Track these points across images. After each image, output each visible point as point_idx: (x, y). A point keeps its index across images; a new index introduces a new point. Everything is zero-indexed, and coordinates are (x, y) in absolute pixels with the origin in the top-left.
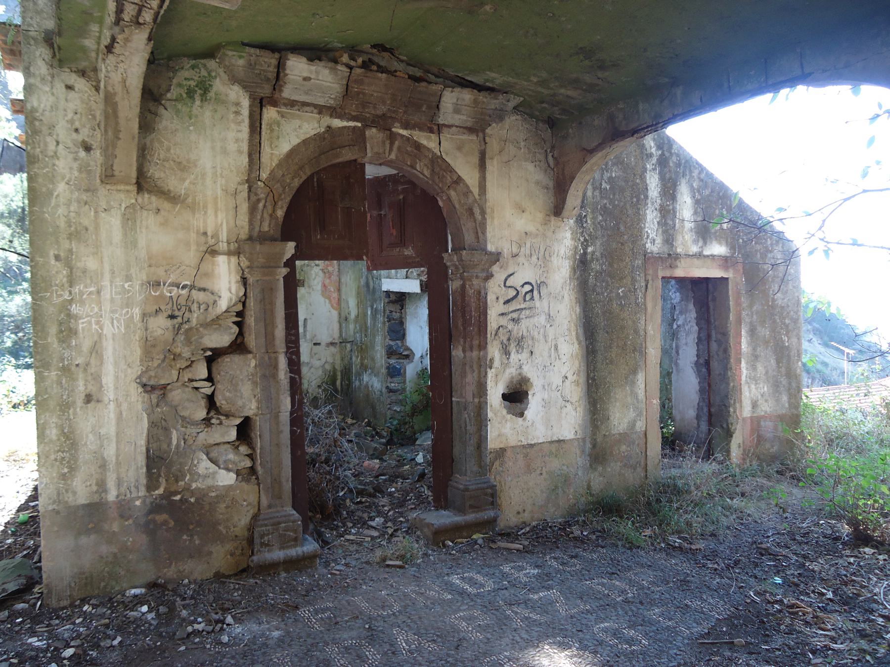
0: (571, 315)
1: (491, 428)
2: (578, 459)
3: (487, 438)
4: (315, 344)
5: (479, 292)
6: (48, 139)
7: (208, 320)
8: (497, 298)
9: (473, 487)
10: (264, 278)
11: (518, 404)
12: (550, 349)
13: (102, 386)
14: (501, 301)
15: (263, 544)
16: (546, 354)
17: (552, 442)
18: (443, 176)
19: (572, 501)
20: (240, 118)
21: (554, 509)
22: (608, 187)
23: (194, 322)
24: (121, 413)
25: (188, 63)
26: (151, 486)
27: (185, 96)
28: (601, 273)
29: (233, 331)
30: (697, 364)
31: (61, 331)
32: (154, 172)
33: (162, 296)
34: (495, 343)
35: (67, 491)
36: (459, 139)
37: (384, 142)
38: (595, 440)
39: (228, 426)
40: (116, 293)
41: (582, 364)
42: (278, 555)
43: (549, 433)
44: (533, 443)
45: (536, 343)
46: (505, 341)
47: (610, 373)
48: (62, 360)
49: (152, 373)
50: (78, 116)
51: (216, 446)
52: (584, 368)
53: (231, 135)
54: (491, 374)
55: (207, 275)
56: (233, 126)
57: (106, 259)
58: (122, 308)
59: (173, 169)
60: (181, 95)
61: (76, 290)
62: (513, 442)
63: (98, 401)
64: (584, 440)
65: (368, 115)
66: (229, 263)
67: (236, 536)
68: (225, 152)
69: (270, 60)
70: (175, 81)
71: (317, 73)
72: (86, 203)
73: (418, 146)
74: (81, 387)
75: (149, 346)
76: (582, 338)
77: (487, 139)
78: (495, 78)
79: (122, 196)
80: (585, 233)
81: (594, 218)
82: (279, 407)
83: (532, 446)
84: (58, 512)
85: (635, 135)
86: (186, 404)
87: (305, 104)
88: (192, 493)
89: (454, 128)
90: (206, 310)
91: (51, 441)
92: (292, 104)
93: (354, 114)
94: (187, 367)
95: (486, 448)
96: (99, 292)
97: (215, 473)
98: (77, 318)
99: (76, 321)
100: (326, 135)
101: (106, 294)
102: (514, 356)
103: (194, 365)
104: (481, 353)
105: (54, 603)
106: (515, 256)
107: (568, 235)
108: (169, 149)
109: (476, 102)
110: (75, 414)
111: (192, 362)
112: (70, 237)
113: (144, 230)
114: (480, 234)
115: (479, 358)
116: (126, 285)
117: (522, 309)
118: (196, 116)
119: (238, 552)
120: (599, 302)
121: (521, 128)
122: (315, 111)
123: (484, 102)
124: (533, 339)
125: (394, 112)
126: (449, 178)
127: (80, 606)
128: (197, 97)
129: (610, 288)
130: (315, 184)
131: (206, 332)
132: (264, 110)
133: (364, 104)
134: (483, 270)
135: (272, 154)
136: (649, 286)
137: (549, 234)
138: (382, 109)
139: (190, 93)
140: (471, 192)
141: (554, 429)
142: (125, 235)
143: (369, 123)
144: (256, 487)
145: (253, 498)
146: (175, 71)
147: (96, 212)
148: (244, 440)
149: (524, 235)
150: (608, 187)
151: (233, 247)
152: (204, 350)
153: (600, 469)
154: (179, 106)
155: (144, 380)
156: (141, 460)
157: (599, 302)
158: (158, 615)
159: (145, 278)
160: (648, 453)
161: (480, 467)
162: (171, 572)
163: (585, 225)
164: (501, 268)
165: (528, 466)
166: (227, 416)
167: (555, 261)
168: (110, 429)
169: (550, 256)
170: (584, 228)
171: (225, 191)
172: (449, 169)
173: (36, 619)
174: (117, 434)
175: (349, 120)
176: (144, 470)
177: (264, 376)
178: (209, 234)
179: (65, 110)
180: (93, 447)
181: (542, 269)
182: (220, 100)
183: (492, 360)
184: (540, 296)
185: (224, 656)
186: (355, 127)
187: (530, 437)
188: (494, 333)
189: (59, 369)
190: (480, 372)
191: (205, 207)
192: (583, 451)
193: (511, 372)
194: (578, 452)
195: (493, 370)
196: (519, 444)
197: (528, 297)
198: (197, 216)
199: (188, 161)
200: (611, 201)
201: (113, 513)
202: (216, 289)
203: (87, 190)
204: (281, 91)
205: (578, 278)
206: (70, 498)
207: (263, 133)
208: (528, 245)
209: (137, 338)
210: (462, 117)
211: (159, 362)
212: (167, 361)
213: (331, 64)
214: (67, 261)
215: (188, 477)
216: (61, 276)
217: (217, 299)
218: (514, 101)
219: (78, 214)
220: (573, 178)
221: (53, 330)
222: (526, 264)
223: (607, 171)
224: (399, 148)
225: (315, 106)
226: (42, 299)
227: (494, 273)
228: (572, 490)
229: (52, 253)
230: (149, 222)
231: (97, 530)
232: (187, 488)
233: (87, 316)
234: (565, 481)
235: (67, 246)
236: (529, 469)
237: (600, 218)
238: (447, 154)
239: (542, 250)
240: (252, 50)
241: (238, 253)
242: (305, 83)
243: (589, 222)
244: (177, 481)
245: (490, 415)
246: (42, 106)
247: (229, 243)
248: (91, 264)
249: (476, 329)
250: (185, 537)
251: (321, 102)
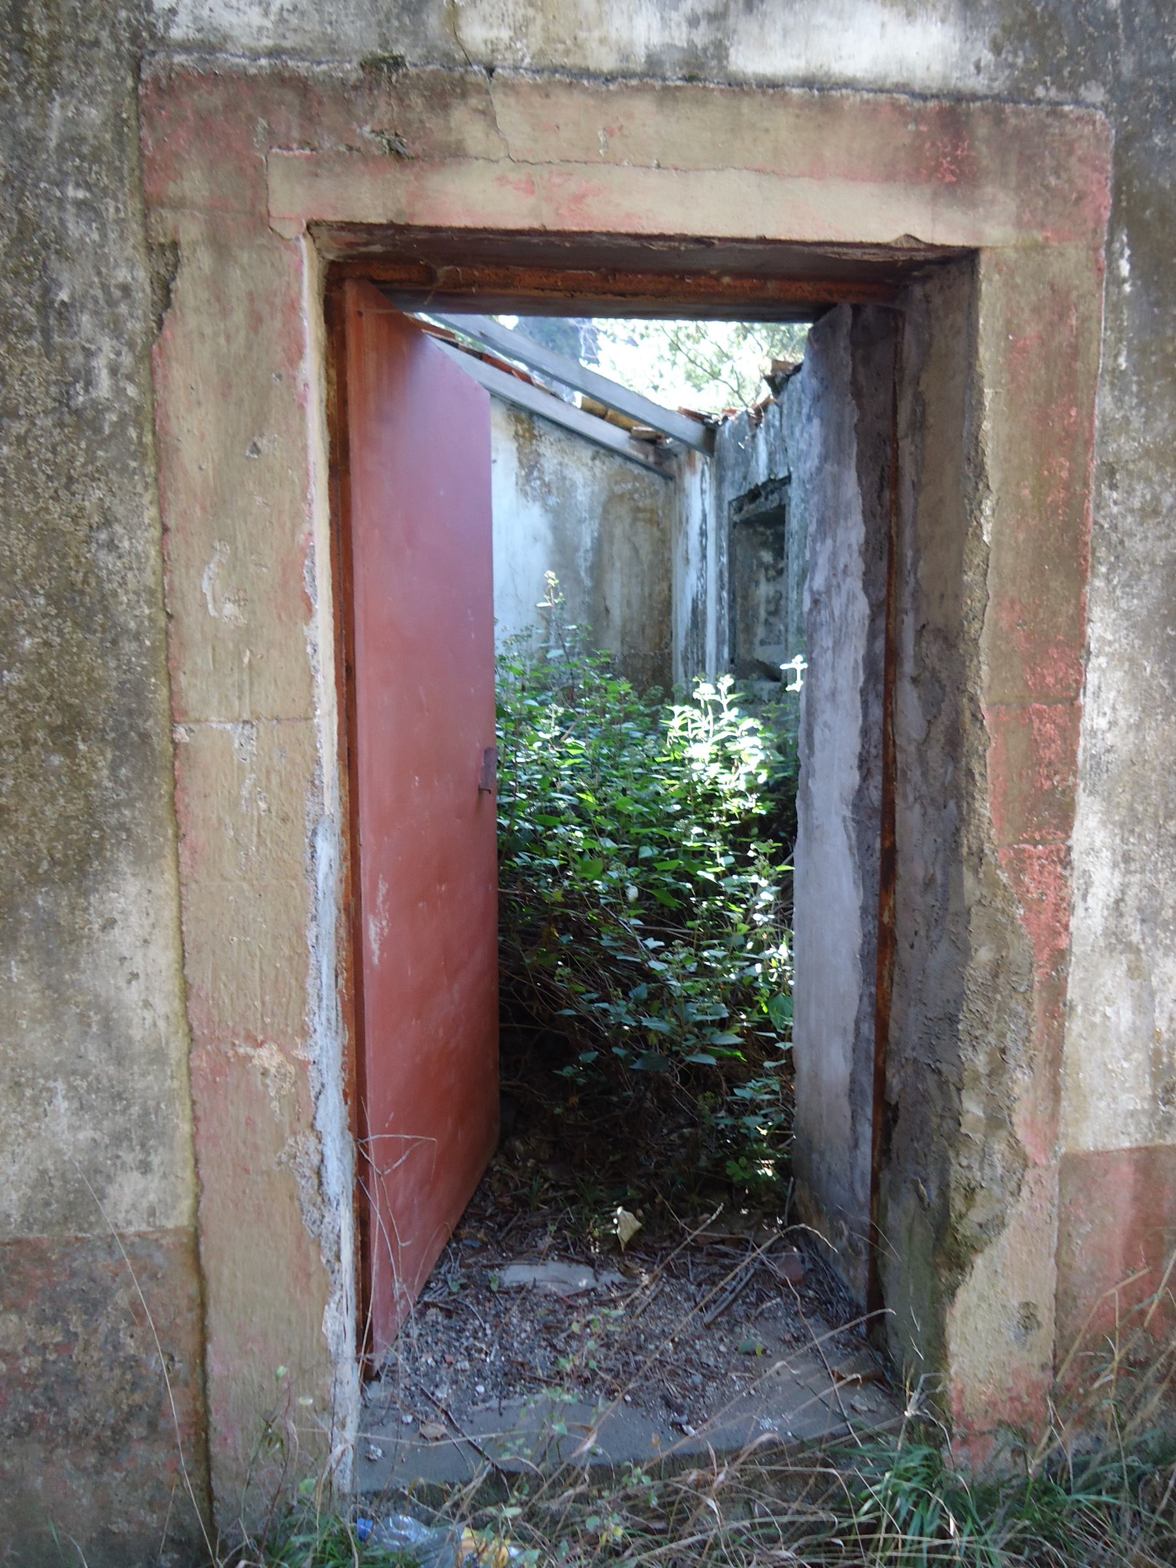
30: (858, 801)
136: (183, 285)
160: (215, 1366)
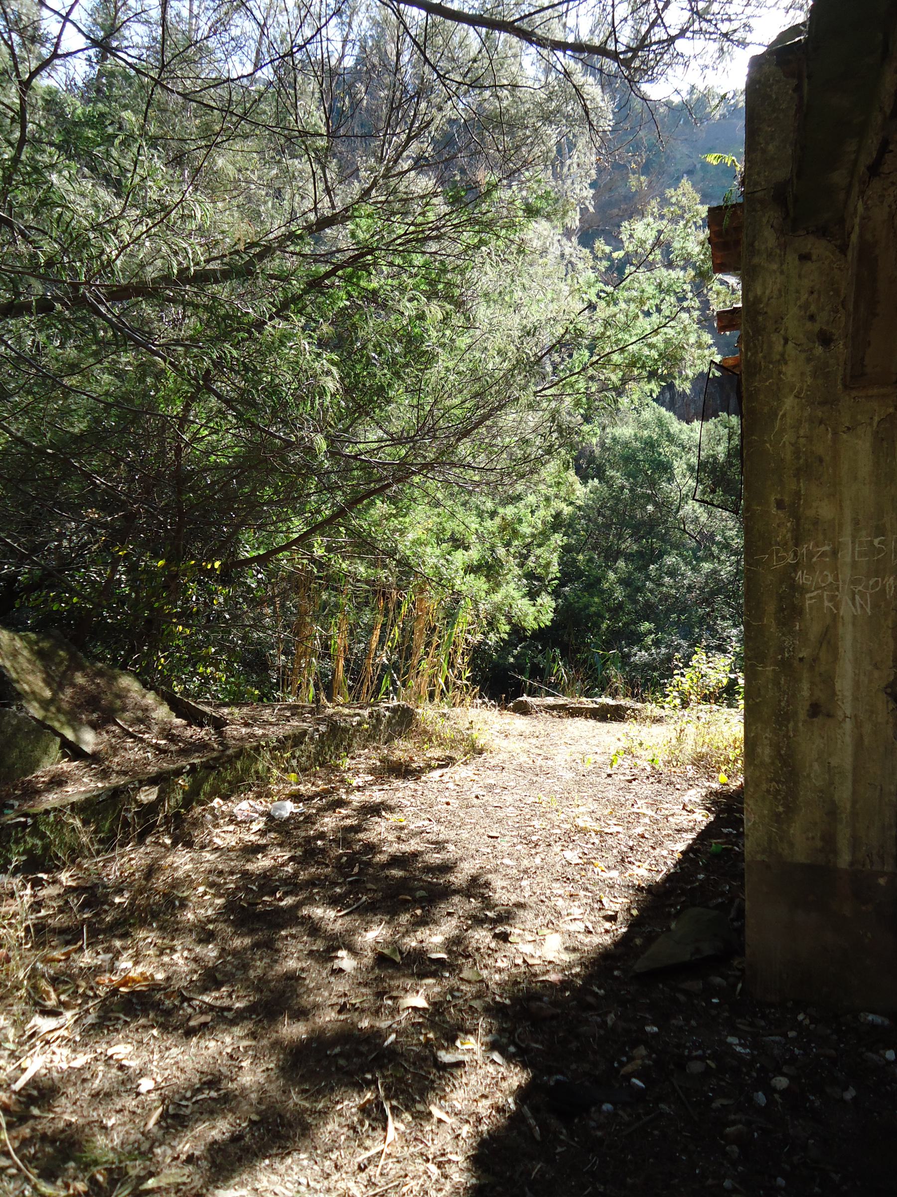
6: (774, 337)
13: (834, 694)
31: (782, 610)
40: (861, 554)
48: (781, 650)
50: (815, 295)
63: (829, 716)
72: (821, 423)
96: (835, 553)
98: (803, 590)
99: (802, 594)
101: (846, 557)
110: (795, 730)
112: (797, 475)
116: (876, 542)
147: (835, 433)
168: (844, 758)
179: (798, 292)
203: (823, 403)
216: (784, 533)
219: (809, 438)
221: (771, 607)
233: (817, 589)
246: (768, 292)
248: (826, 511)
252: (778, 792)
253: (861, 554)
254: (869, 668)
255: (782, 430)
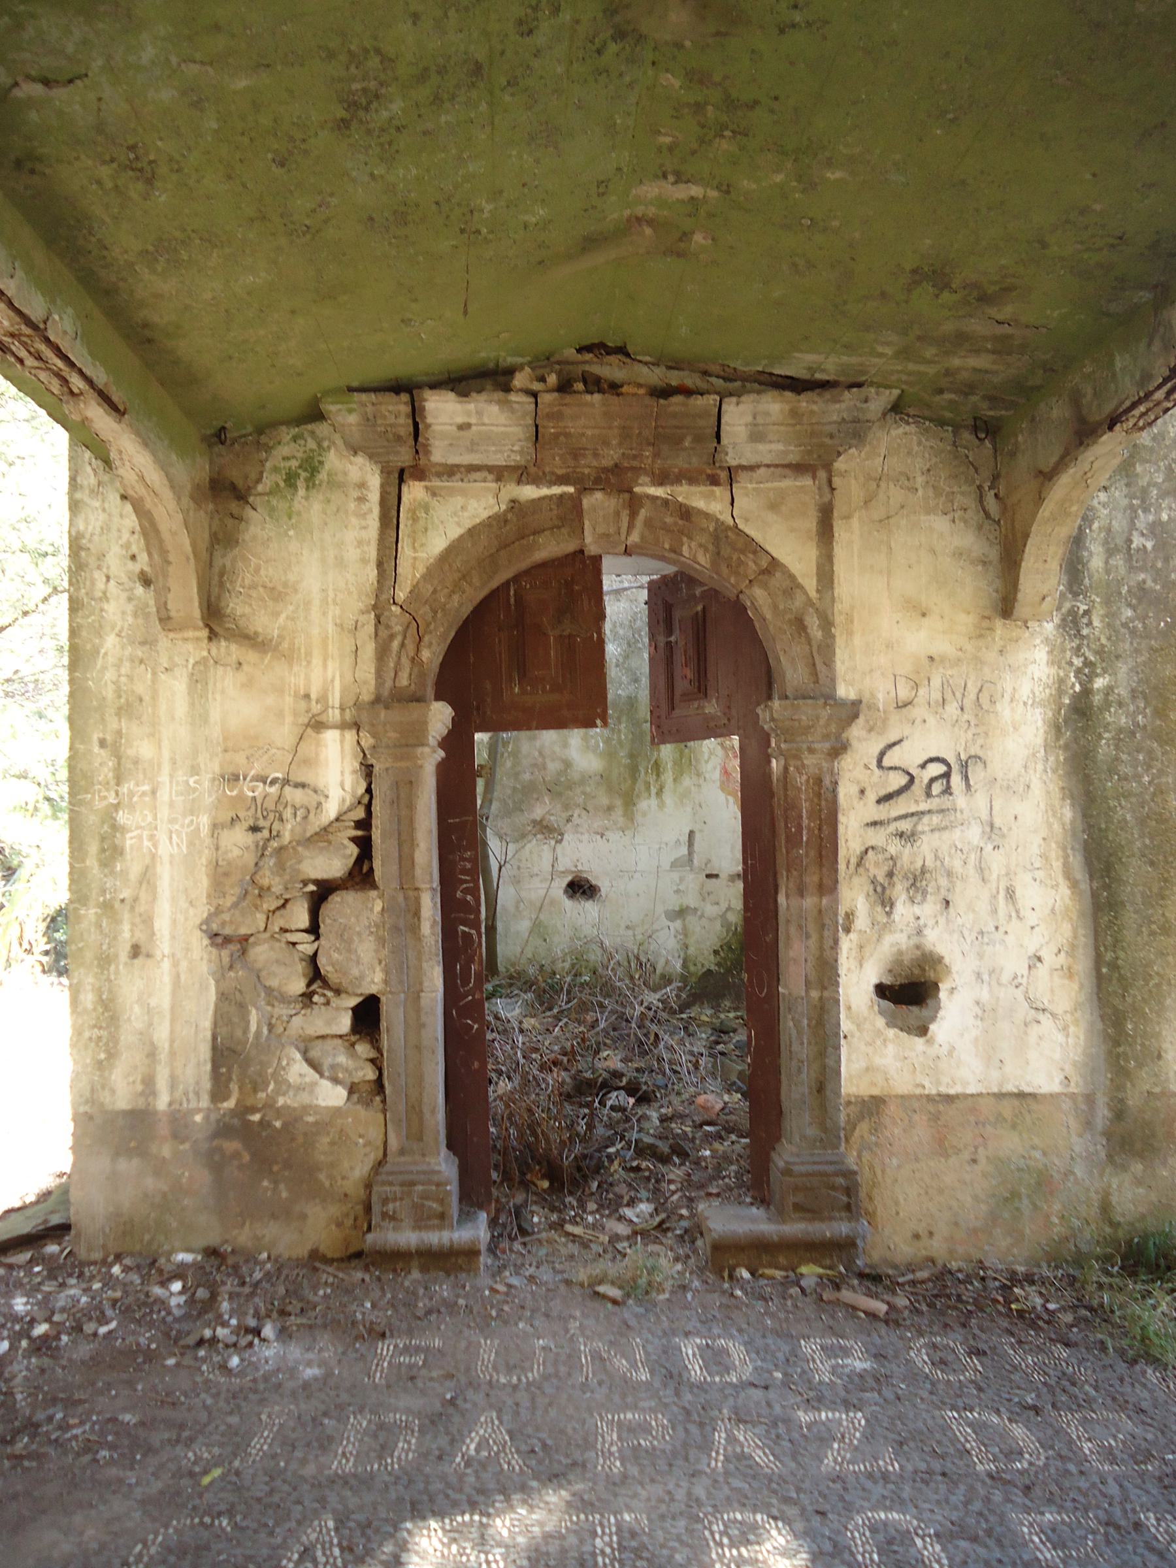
0: (1050, 826)
1: (849, 1054)
2: (1074, 1139)
3: (839, 1073)
4: (709, 876)
5: (819, 781)
7: (308, 834)
8: (862, 792)
9: (803, 1169)
10: (399, 764)
11: (914, 1009)
12: (995, 897)
13: (153, 934)
14: (872, 796)
15: (385, 1215)
16: (983, 906)
17: (1000, 1096)
18: (740, 563)
19: (1058, 1230)
20: (365, 507)
21: (1009, 1240)
22: (1149, 545)
23: (287, 837)
24: (178, 976)
25: (286, 433)
26: (218, 1094)
27: (282, 484)
28: (1133, 734)
29: (348, 852)
31: (103, 850)
32: (235, 606)
33: (241, 797)
34: (856, 881)
35: (103, 1087)
36: (774, 489)
37: (617, 514)
38: (1122, 1101)
39: (337, 1009)
40: (179, 794)
41: (1081, 931)
42: (407, 1238)
43: (995, 1075)
44: (952, 1092)
45: (958, 883)
46: (880, 879)
47: (1162, 954)
48: (103, 892)
49: (226, 917)
51: (320, 1041)
52: (1085, 940)
53: (350, 536)
54: (847, 944)
55: (308, 762)
56: (354, 520)
57: (166, 744)
58: (184, 816)
59: (263, 599)
60: (277, 485)
61: (124, 789)
62: (902, 1084)
63: (148, 956)
64: (1090, 1099)
65: (586, 471)
66: (342, 742)
67: (346, 1195)
68: (340, 563)
69: (396, 408)
70: (268, 465)
71: (479, 413)
72: (141, 661)
73: (686, 513)
74: (126, 935)
75: (220, 874)
76: (1080, 874)
77: (837, 481)
78: (829, 365)
79: (190, 646)
80: (1085, 650)
81: (1111, 616)
82: (421, 984)
83: (949, 1099)
84: (91, 1118)
85: (1118, 427)
86: (274, 968)
87: (472, 468)
88: (279, 1112)
89: (762, 470)
90: (305, 818)
91: (85, 1010)
92: (450, 471)
93: (560, 472)
94: (278, 908)
95: (838, 1094)
96: (154, 792)
97: (314, 1084)
98: (123, 830)
99: (123, 834)
100: (509, 516)
101: (164, 795)
102: (903, 911)
103: (288, 906)
104: (824, 901)
105: (82, 1254)
106: (903, 705)
107: (1041, 654)
108: (257, 570)
109: (794, 413)
110: (117, 972)
111: (287, 901)
112: (120, 711)
113: (218, 697)
114: (820, 666)
115: (820, 911)
117: (923, 813)
118: (299, 514)
119: (349, 1222)
120: (1127, 795)
121: (916, 448)
122: (490, 477)
123: (812, 412)
124: (949, 874)
125: (635, 457)
126: (751, 564)
127: (111, 1266)
128: (301, 484)
129: (1159, 765)
130: (512, 600)
131: (306, 853)
132: (405, 488)
133: (576, 454)
134: (826, 737)
135: (415, 559)
137: (991, 656)
138: (611, 456)
139: (291, 479)
140: (800, 587)
141: (1008, 1069)
142: (192, 705)
143: (589, 484)
144: (381, 1117)
145: (375, 1133)
146: (268, 449)
147: (154, 674)
148: (368, 1034)
149: (926, 662)
150: (1149, 545)
151: (348, 716)
152: (305, 883)
153: (1138, 1167)
154: (274, 502)
155: (215, 927)
156: (204, 1052)
157: (1127, 795)
158: (191, 1301)
159: (217, 769)
161: (825, 1130)
162: (243, 1237)
163: (1085, 632)
164: (871, 730)
165: (941, 1141)
166: (338, 992)
167: (1004, 710)
168: (163, 999)
169: (993, 702)
170: (1083, 637)
171: (340, 626)
172: (753, 547)
173: (53, 1272)
174: (173, 1008)
175: (551, 484)
176: (209, 1067)
177: (396, 929)
178: (313, 696)
180: (138, 1025)
181: (973, 730)
182: (335, 484)
183: (850, 916)
184: (968, 786)
185: (207, 1391)
186: (561, 497)
187: (945, 1080)
188: (854, 861)
189: (99, 906)
190: (822, 937)
191: (309, 654)
192: (1088, 1124)
193: (897, 941)
194: (1073, 1123)
195: (852, 936)
196: (918, 1091)
197: (937, 788)
198: (296, 669)
199: (285, 585)
200: (1158, 575)
201: (163, 1129)
202: (321, 785)
203: (143, 643)
204: (428, 453)
205: (1066, 747)
206: (105, 1097)
207: (401, 526)
208: (936, 682)
209: (204, 861)
210: (774, 447)
211: (234, 899)
212: (249, 897)
213: (500, 395)
214: (114, 747)
215: (271, 1087)
216: (106, 773)
217: (323, 800)
218: (880, 401)
219: (130, 678)
220: (1026, 536)
221: (93, 848)
222: (932, 721)
223: (1146, 510)
224: (648, 523)
225: (490, 469)
226: (81, 803)
227: (854, 743)
228: (1057, 1207)
229: (95, 737)
230: (226, 681)
231: (141, 1152)
232: (269, 1105)
233: (138, 828)
234: (1039, 1184)
235: (115, 726)
236: (942, 1147)
237: (1129, 613)
238: (747, 520)
239: (972, 690)
240: (364, 397)
241: (357, 726)
242: (462, 433)
243: (1096, 623)
244: (255, 1090)
245: (846, 1026)
246: (90, 528)
247: (342, 709)
249: (812, 853)
250: (265, 1183)
251: (499, 460)
252: (100, 1038)
253: (179, 794)
254: (185, 905)
255: (104, 668)
